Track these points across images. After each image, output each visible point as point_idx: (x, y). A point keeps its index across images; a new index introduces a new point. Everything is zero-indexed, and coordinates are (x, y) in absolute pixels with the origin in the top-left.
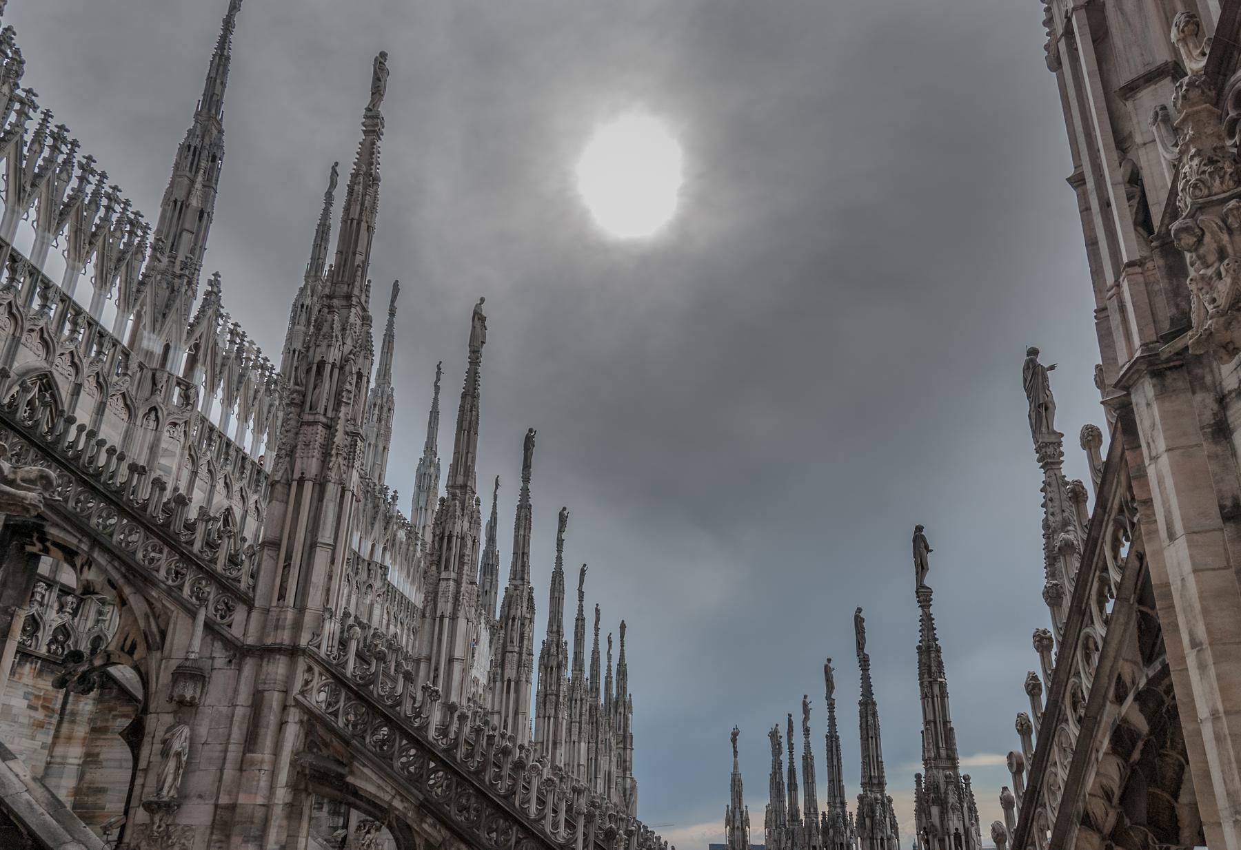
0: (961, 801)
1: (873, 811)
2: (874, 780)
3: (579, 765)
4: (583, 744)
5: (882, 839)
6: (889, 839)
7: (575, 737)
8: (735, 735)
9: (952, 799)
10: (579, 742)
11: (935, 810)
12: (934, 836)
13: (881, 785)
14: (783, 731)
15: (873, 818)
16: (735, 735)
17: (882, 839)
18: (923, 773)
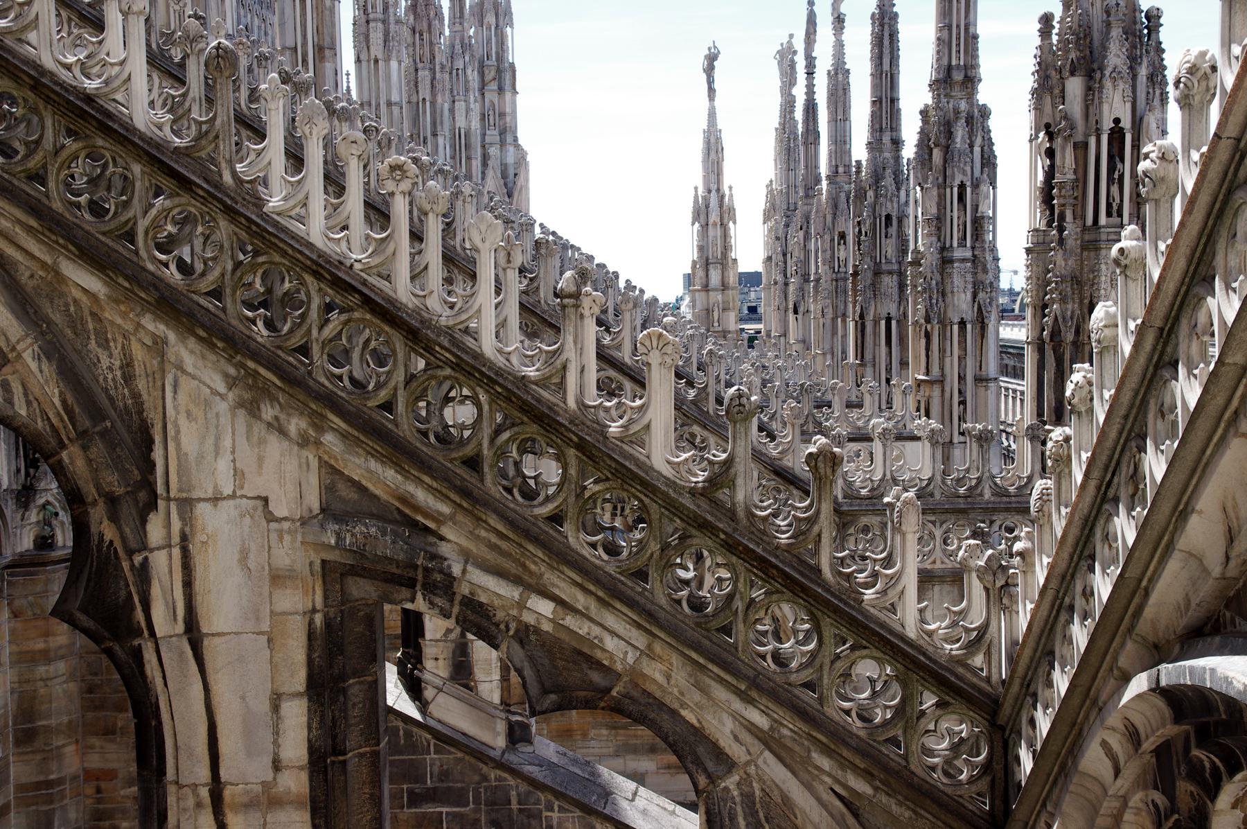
0: (1134, 61)
1: (950, 135)
2: (957, 73)
3: (389, 104)
4: (394, 64)
5: (962, 187)
6: (976, 186)
7: (377, 50)
8: (712, 59)
9: (1116, 57)
10: (387, 60)
11: (1075, 86)
12: (1066, 139)
13: (970, 81)
14: (799, 45)
15: (947, 149)
16: (712, 59)
17: (962, 187)
18: (1058, 11)
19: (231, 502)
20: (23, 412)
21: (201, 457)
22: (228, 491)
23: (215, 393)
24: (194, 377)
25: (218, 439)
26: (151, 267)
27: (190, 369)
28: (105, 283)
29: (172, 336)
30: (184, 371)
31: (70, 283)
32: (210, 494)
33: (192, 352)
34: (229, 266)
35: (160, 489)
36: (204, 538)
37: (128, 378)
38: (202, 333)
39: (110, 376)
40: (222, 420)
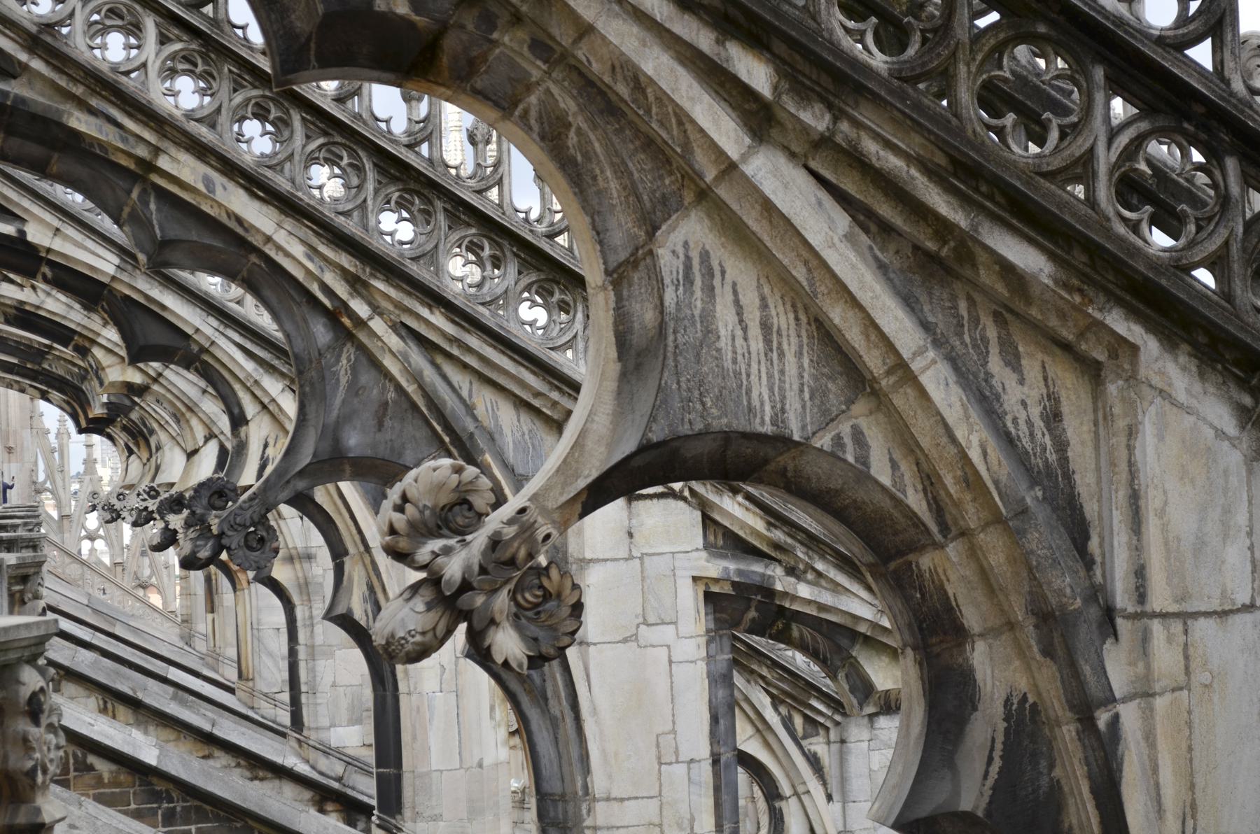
19: (1247, 618)
20: (885, 480)
21: (1200, 545)
22: (1243, 598)
23: (1220, 434)
24: (1189, 411)
25: (1227, 511)
26: (1121, 229)
27: (1182, 397)
28: (1052, 256)
29: (1150, 346)
30: (1174, 403)
31: (982, 257)
32: (1215, 605)
33: (1184, 369)
34: (1240, 230)
35: (1122, 599)
36: (1205, 677)
37: (1053, 417)
38: (1202, 339)
39: (1022, 416)
40: (1234, 480)
